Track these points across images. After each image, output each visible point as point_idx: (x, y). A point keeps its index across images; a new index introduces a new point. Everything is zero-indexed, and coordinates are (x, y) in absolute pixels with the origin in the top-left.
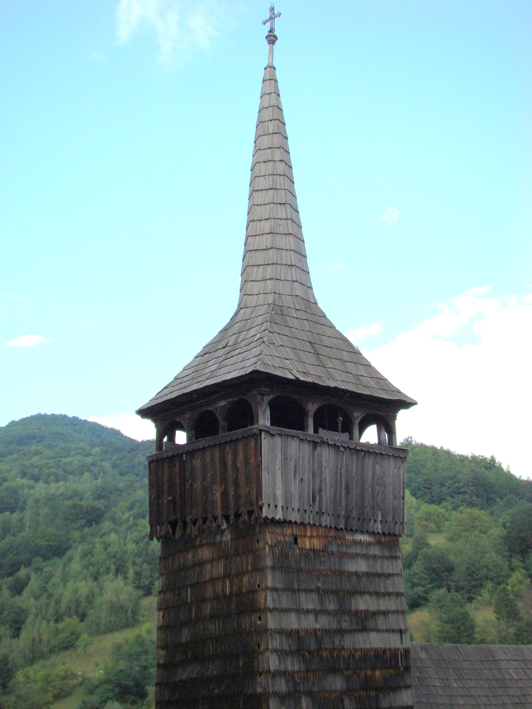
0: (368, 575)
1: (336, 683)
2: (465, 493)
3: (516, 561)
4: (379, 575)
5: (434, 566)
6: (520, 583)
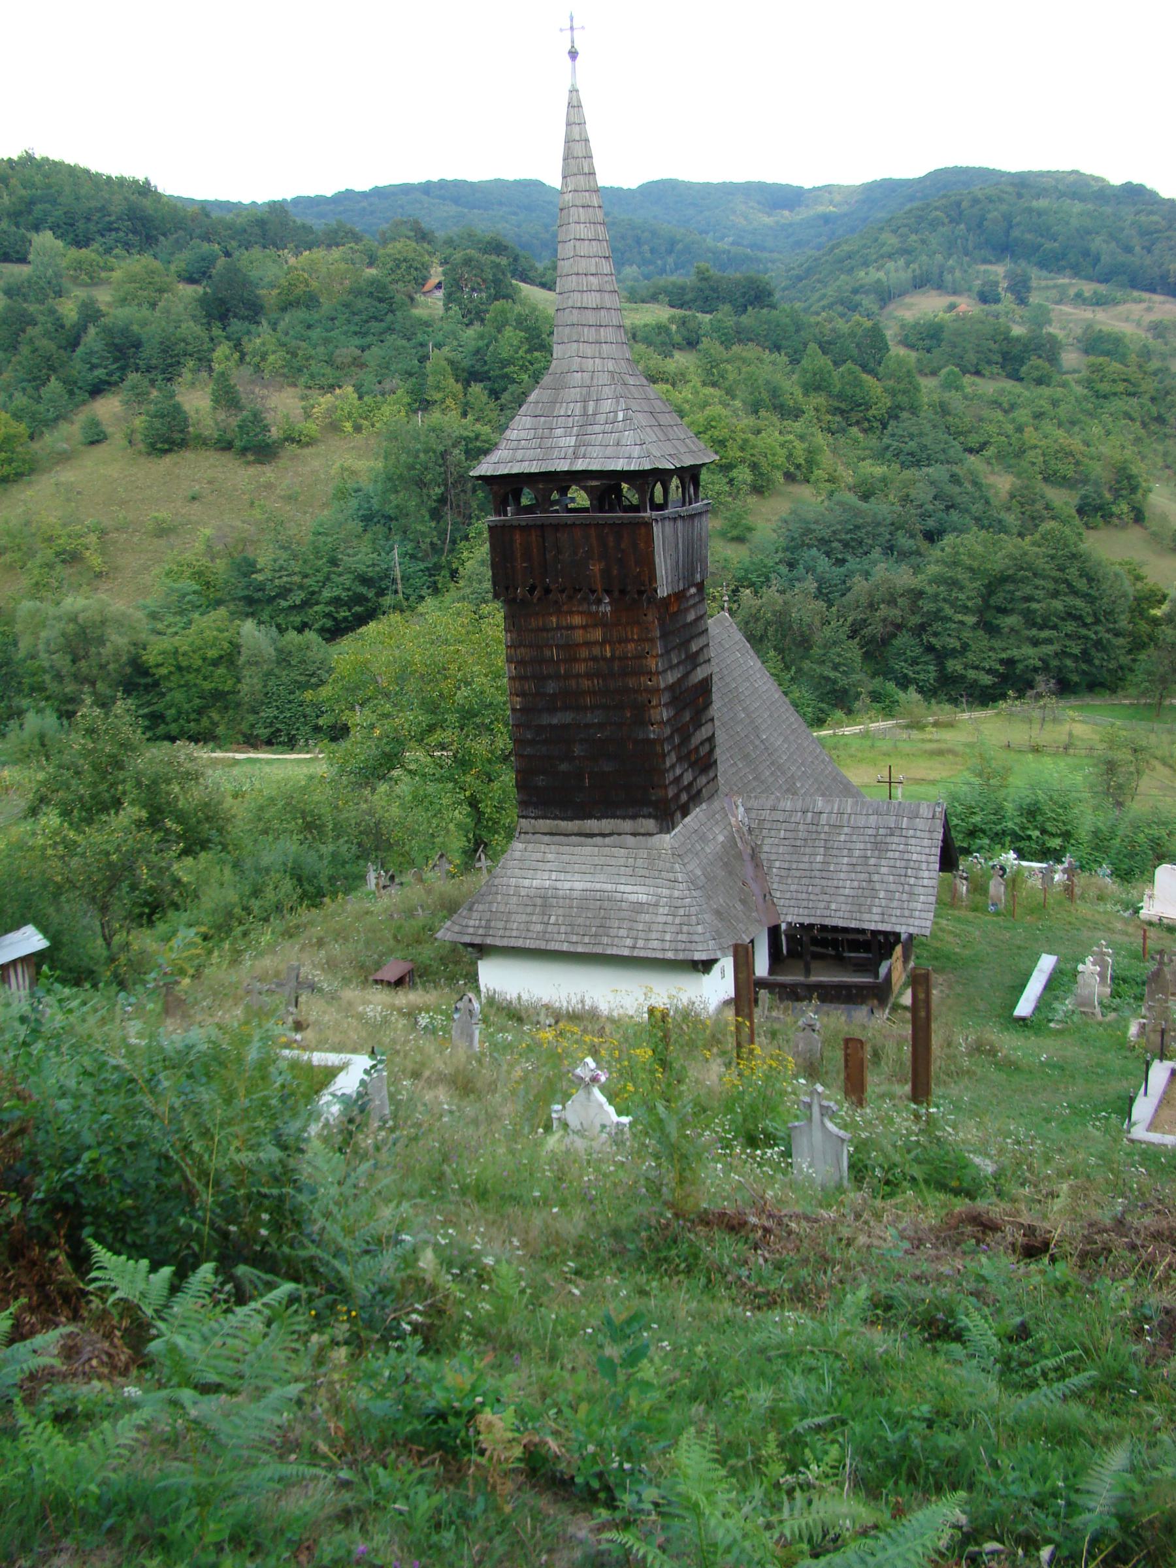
2: (117, 230)
3: (216, 332)
5: (117, 341)
6: (227, 359)
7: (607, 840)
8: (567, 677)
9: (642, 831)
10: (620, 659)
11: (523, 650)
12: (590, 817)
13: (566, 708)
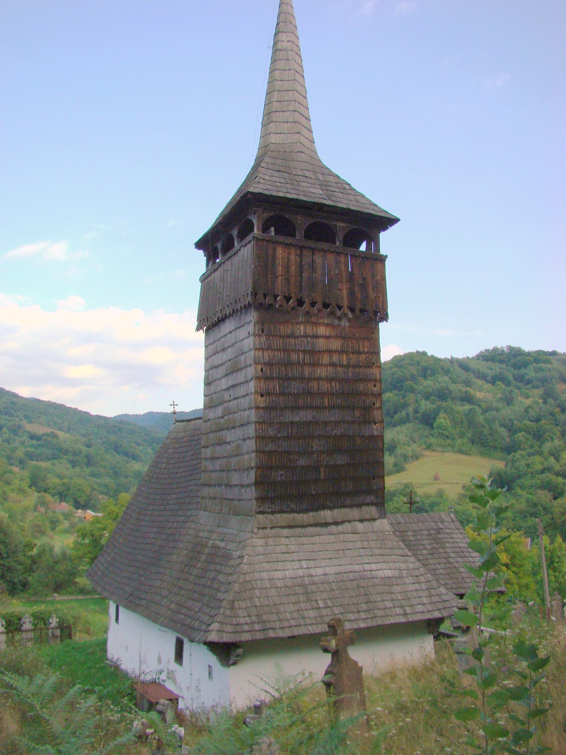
7: (340, 528)
8: (310, 379)
9: (367, 517)
10: (354, 366)
11: (271, 353)
12: (323, 508)
13: (306, 408)
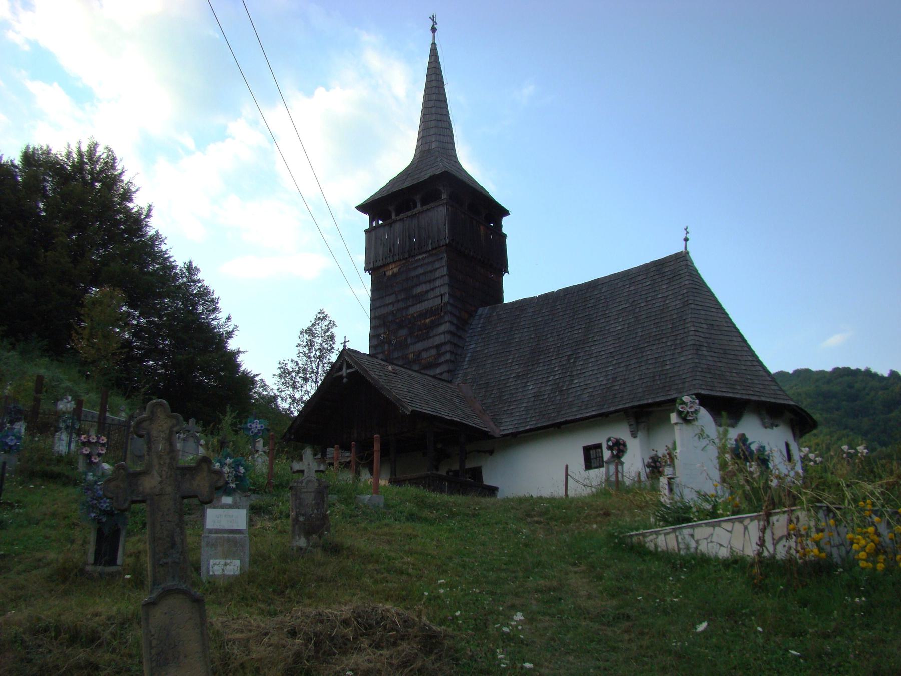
0: (424, 274)
1: (404, 332)
4: (431, 272)
